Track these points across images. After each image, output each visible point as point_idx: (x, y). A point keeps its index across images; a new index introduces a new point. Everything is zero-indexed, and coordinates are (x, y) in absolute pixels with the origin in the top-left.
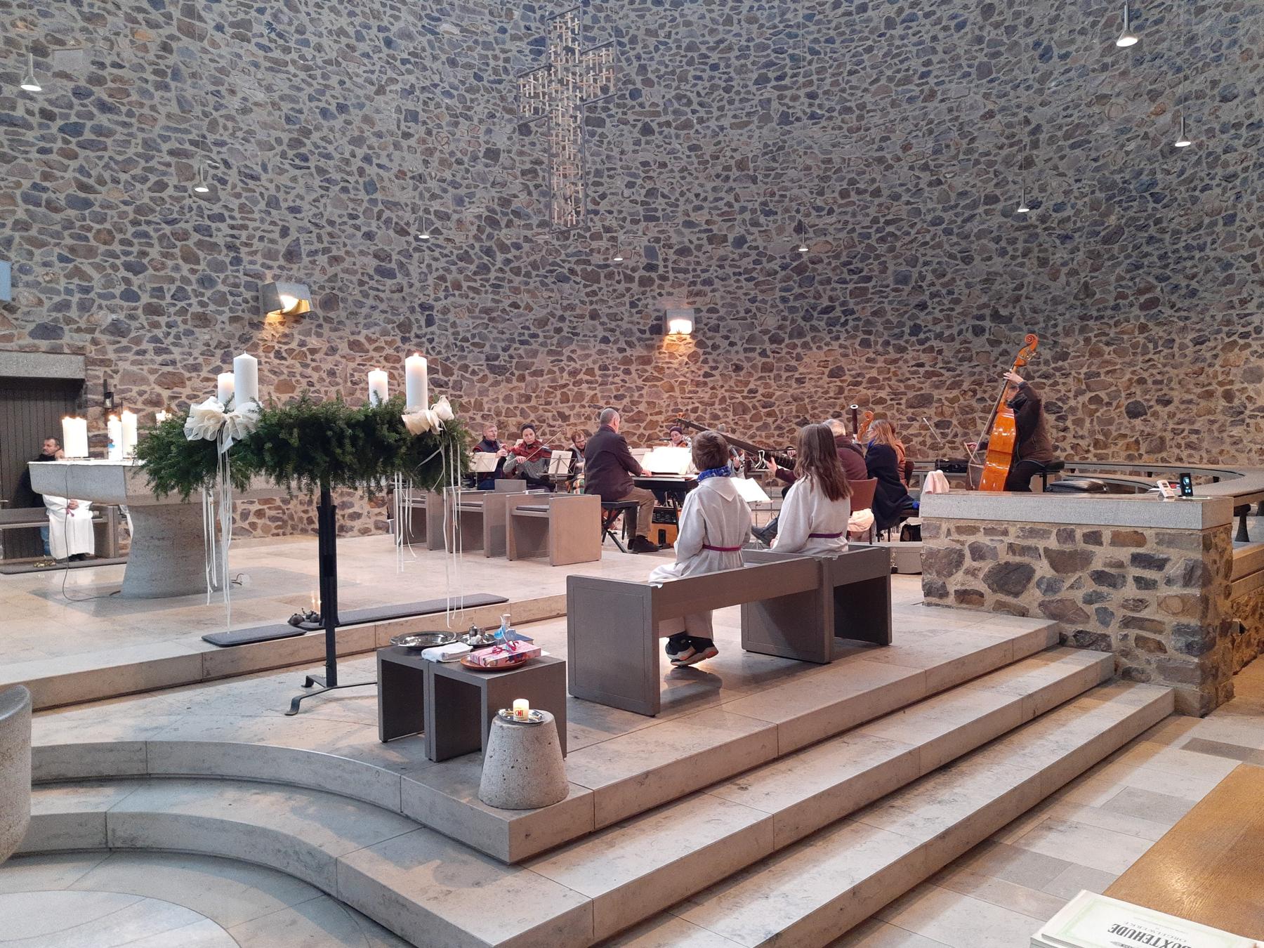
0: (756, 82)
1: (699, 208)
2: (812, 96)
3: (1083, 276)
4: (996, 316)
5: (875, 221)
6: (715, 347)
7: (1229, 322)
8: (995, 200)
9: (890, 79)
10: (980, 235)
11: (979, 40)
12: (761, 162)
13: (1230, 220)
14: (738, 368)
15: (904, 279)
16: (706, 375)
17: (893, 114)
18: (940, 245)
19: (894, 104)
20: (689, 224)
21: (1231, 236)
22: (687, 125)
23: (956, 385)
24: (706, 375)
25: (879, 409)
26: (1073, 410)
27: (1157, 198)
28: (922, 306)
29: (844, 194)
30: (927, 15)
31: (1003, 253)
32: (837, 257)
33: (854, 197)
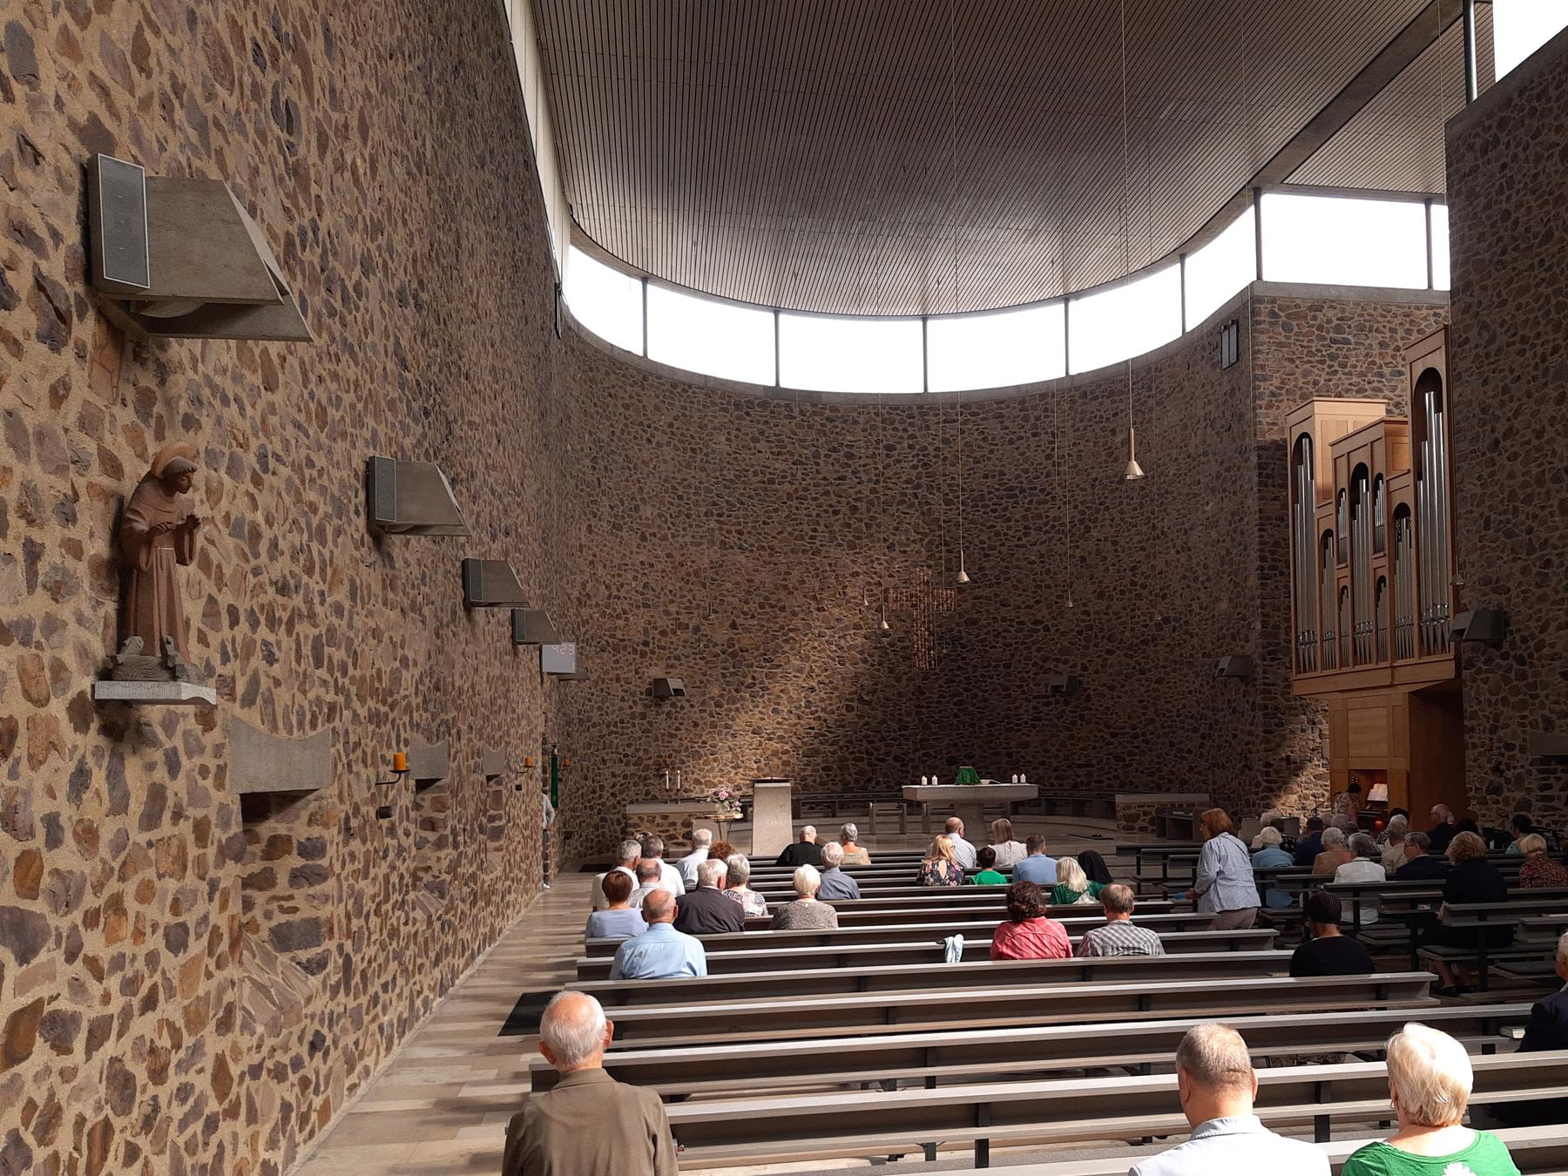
0: (706, 514)
1: (672, 602)
2: (740, 533)
3: (918, 682)
4: (861, 699)
5: (782, 628)
6: (682, 708)
7: (1007, 717)
8: (859, 627)
9: (791, 534)
10: (850, 648)
11: (849, 526)
12: (710, 573)
13: (1007, 666)
14: (696, 725)
15: (800, 670)
16: (678, 729)
17: (792, 558)
18: (824, 650)
19: (793, 551)
20: (667, 613)
21: (1009, 674)
22: (665, 538)
23: (835, 743)
24: (678, 729)
25: (785, 757)
26: (912, 760)
27: (964, 647)
28: (812, 689)
29: (761, 606)
30: (814, 499)
31: (865, 661)
32: (757, 649)
33: (768, 609)
